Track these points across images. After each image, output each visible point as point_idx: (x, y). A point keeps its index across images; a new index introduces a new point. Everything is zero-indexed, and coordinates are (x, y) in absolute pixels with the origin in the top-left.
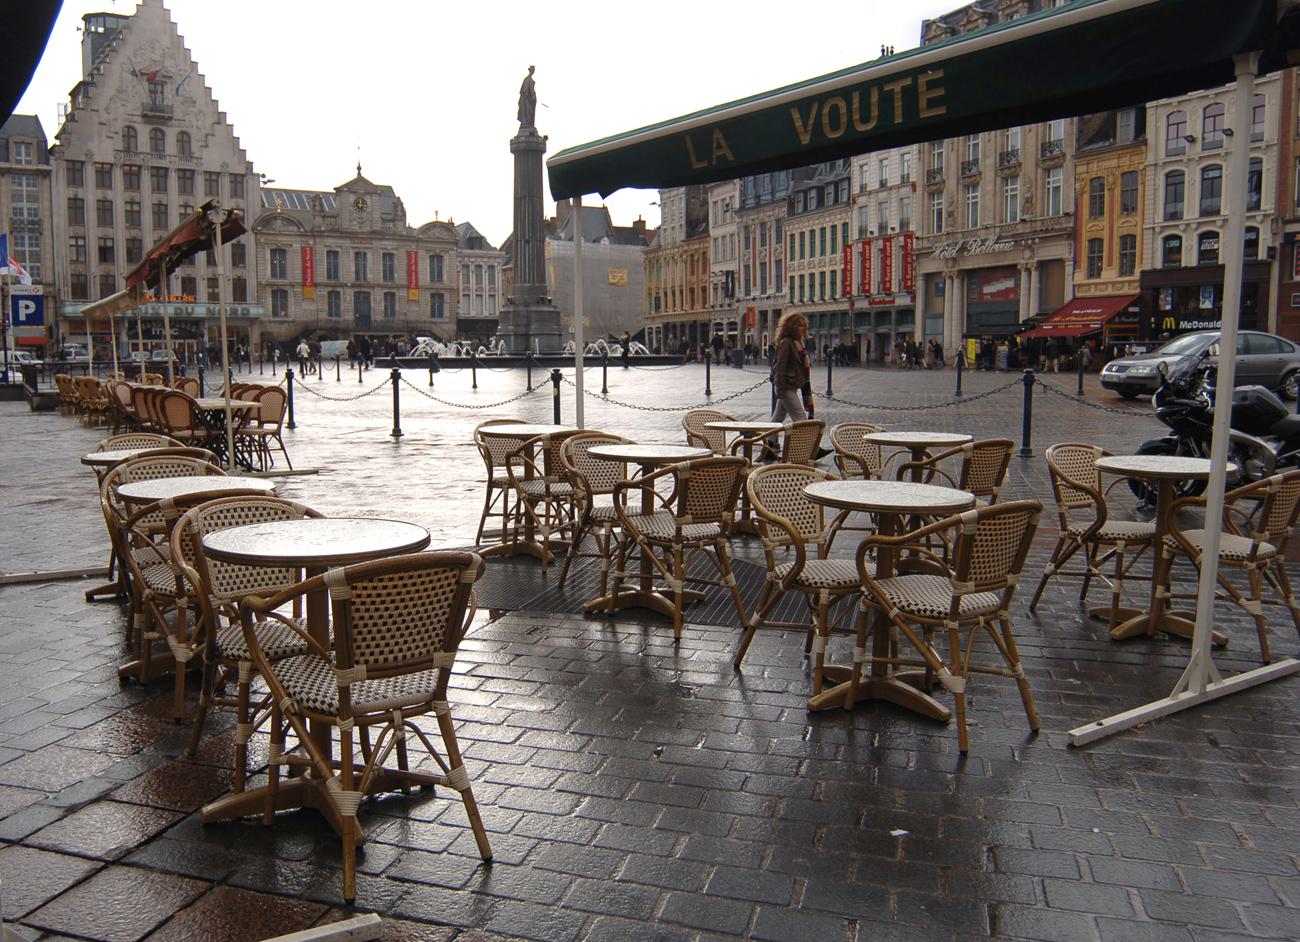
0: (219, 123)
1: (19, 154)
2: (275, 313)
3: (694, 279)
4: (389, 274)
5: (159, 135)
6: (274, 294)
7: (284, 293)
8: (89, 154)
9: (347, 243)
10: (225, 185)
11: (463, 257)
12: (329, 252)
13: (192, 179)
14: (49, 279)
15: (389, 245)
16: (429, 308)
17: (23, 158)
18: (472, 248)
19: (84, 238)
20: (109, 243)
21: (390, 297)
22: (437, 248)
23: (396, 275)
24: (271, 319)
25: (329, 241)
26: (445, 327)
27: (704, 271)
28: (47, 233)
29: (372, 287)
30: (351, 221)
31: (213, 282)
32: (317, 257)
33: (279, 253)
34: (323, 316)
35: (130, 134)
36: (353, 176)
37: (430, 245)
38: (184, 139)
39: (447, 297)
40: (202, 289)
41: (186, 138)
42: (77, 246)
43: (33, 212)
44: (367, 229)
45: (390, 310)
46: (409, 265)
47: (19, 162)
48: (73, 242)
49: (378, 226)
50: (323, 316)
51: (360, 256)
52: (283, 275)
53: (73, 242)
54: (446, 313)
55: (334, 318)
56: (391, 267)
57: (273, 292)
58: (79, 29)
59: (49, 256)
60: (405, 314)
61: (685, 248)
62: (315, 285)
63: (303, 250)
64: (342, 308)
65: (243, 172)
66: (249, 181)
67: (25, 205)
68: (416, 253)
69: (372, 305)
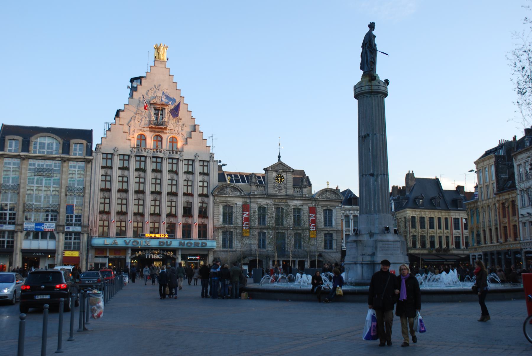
0: (195, 131)
1: (75, 150)
2: (224, 246)
3: (506, 220)
5: (159, 139)
6: (224, 233)
9: (270, 202)
11: (345, 210)
15: (298, 203)
18: (351, 205)
19: (109, 198)
24: (222, 249)
25: (260, 201)
26: (333, 255)
27: (514, 214)
28: (87, 195)
30: (274, 188)
34: (255, 247)
35: (142, 138)
36: (276, 161)
37: (324, 203)
39: (335, 236)
40: (179, 233)
41: (175, 140)
44: (283, 193)
54: (334, 246)
57: (223, 232)
58: (128, 87)
61: (498, 199)
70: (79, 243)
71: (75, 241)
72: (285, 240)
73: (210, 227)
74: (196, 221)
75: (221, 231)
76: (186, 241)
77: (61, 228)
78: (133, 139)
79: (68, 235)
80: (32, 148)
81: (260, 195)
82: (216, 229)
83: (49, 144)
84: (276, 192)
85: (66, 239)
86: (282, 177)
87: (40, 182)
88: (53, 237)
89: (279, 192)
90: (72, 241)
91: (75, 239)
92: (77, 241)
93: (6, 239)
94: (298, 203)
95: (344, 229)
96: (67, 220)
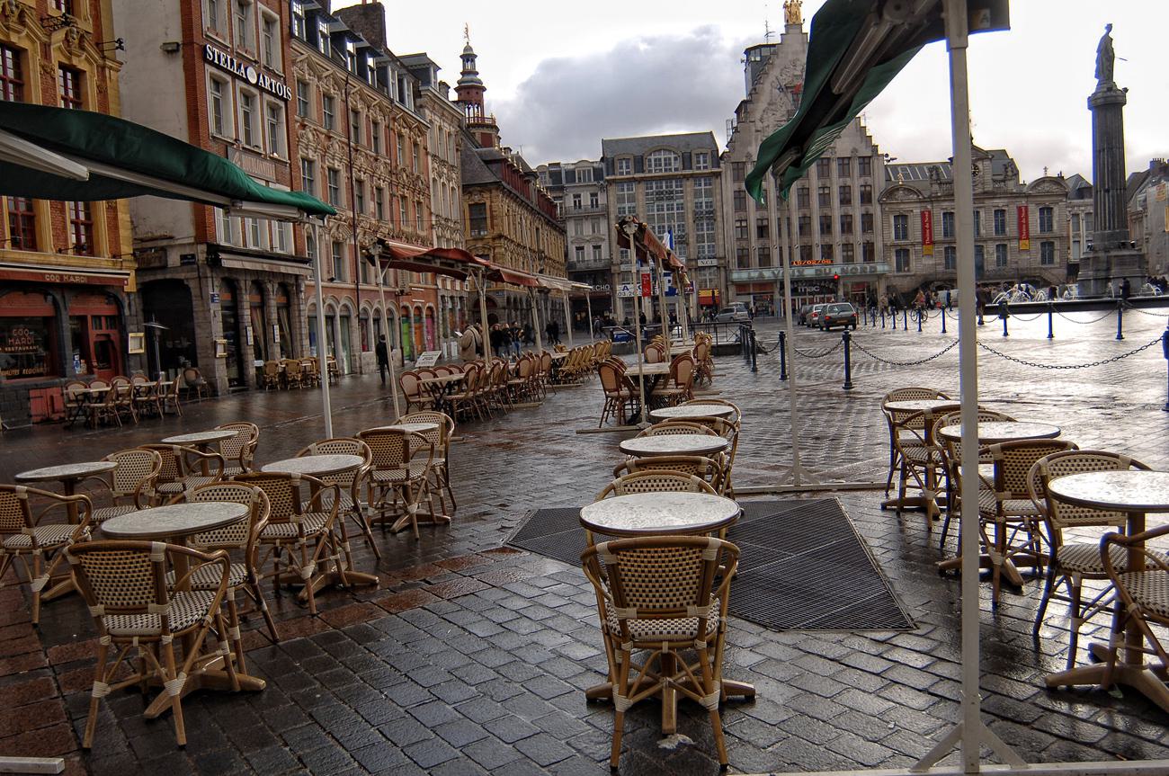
1: (698, 162)
2: (899, 269)
4: (1001, 227)
10: (856, 167)
13: (828, 165)
14: (721, 255)
15: (1000, 203)
17: (702, 165)
18: (1082, 198)
20: (765, 223)
21: (1002, 248)
22: (1047, 201)
23: (1007, 229)
26: (1055, 272)
28: (719, 219)
29: (985, 241)
31: (848, 247)
32: (935, 219)
33: (902, 218)
34: (941, 268)
37: (1039, 199)
39: (1057, 245)
40: (838, 253)
42: (741, 227)
43: (709, 204)
45: (1002, 260)
46: (1020, 219)
47: (699, 168)
48: (738, 224)
49: (989, 187)
50: (941, 268)
52: (905, 237)
53: (738, 224)
54: (1057, 259)
55: (950, 270)
56: (1003, 222)
57: (897, 251)
59: (721, 237)
60: (1017, 263)
62: (932, 243)
63: (923, 214)
66: (875, 163)
67: (704, 200)
68: (1026, 207)
73: (878, 246)
74: (858, 237)
76: (850, 267)
80: (646, 167)
81: (945, 196)
83: (665, 159)
94: (1000, 203)
95: (1071, 234)
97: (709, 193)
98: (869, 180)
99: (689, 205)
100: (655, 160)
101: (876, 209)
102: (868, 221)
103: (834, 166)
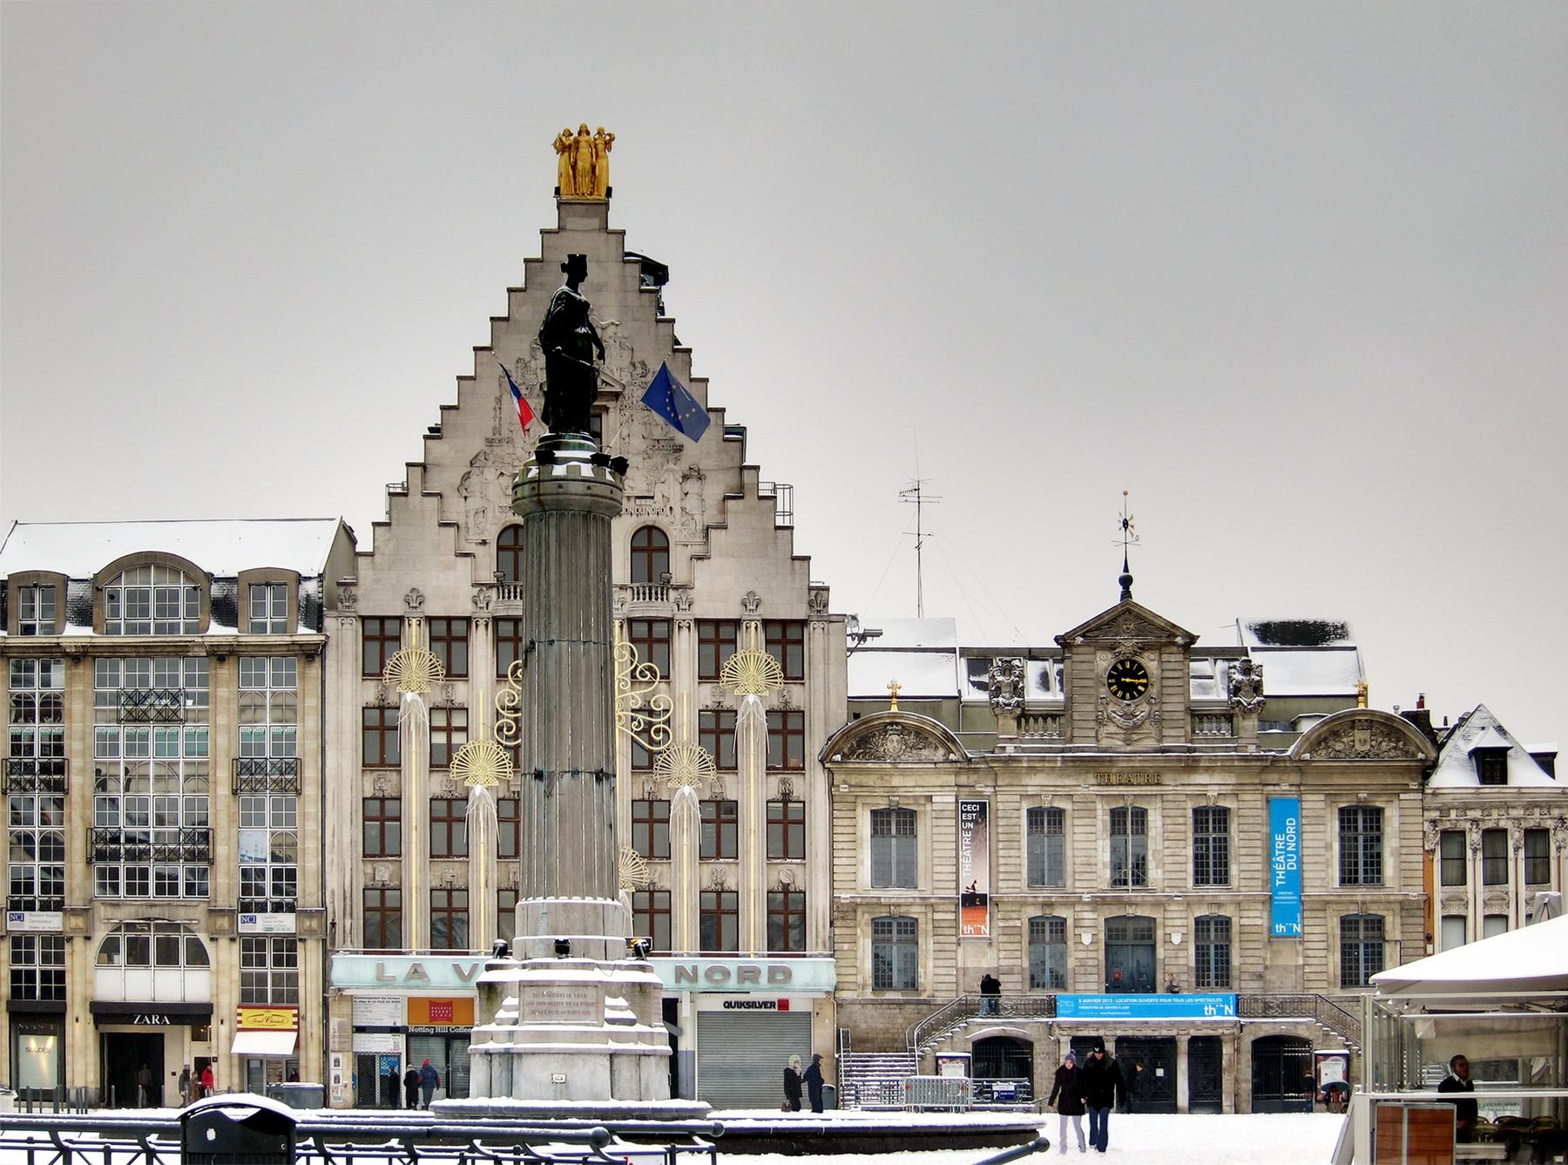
2: (882, 980)
6: (881, 928)
7: (909, 927)
8: (415, 598)
9: (1086, 786)
12: (1035, 816)
13: (667, 641)
16: (1336, 958)
23: (1234, 870)
25: (1034, 783)
28: (311, 790)
33: (896, 822)
36: (1113, 598)
38: (651, 544)
41: (657, 541)
47: (261, 628)
51: (1128, 821)
56: (1222, 848)
60: (1260, 977)
64: (1071, 963)
65: (800, 612)
69: (1161, 953)
70: (293, 979)
71: (279, 970)
72: (1153, 947)
75: (867, 917)
77: (224, 922)
78: (478, 550)
79: (252, 948)
82: (841, 913)
83: (161, 595)
84: (1111, 740)
85: (246, 961)
86: (1137, 670)
87: (137, 745)
88: (198, 957)
89: (1128, 742)
90: (269, 969)
91: (278, 961)
92: (285, 970)
93: (38, 966)
95: (1439, 892)
96: (246, 890)
97: (287, 710)
98: (796, 696)
99: (222, 740)
100: (131, 595)
101: (813, 788)
102: (787, 826)
103: (685, 645)
